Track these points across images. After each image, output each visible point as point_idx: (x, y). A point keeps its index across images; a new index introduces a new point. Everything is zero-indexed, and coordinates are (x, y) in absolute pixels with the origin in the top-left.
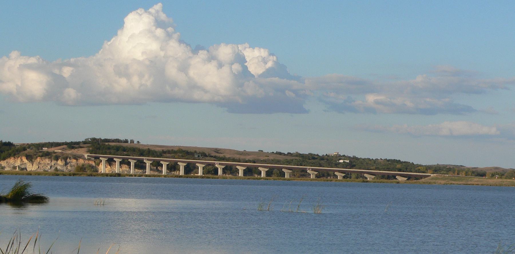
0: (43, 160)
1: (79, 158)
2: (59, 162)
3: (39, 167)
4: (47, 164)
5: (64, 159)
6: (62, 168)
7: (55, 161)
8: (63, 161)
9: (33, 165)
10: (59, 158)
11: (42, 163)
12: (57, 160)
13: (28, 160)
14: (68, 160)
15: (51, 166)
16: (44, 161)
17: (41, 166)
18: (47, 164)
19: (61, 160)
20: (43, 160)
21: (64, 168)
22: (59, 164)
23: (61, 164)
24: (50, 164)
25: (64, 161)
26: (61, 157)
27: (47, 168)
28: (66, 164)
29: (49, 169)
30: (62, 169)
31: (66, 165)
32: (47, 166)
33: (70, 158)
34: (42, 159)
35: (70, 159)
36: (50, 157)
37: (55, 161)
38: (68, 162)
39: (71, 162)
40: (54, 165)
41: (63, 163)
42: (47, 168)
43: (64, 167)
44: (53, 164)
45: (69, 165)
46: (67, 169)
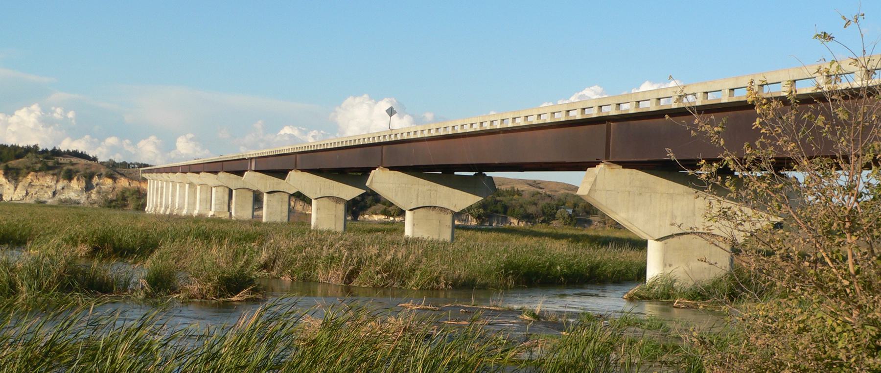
0: (41, 179)
1: (119, 176)
2: (75, 184)
3: (27, 194)
4: (47, 187)
5: (85, 177)
6: (79, 196)
7: (66, 182)
8: (81, 182)
9: (15, 190)
10: (74, 175)
11: (37, 185)
12: (70, 178)
13: (6, 178)
14: (96, 180)
15: (56, 191)
17: (32, 191)
18: (47, 187)
19: (78, 179)
20: (39, 179)
21: (83, 197)
22: (73, 187)
23: (77, 187)
24: (54, 187)
25: (84, 181)
28: (88, 188)
29: (50, 198)
30: (79, 198)
32: (46, 192)
33: (100, 176)
34: (38, 177)
35: (98, 178)
36: (56, 171)
37: (65, 181)
38: (94, 185)
40: (63, 188)
41: (80, 186)
42: (46, 196)
44: (59, 187)
45: (94, 191)
46: (88, 198)
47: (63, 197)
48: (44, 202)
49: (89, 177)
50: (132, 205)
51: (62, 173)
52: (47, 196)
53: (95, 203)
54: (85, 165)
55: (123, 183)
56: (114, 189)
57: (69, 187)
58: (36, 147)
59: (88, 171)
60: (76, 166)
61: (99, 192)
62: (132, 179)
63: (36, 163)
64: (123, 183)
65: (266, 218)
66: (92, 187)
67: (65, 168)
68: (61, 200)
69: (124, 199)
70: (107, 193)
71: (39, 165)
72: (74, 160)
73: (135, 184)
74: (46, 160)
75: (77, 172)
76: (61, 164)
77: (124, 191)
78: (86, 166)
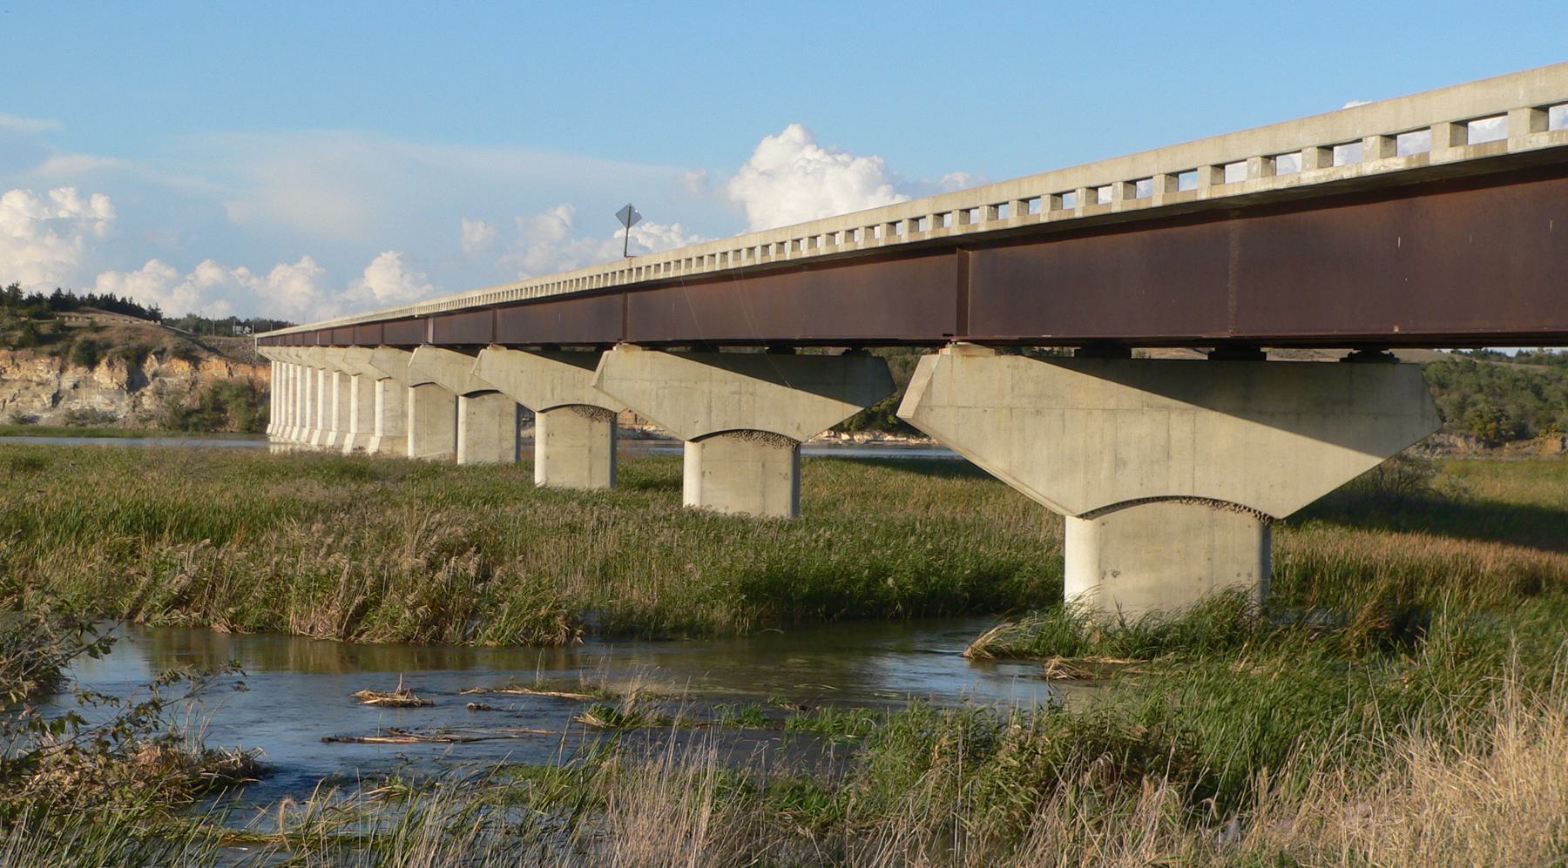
0: (23, 364)
1: (204, 354)
2: (102, 374)
4: (39, 384)
5: (127, 358)
6: (112, 402)
7: (82, 370)
8: (117, 370)
10: (99, 354)
11: (15, 380)
12: (91, 363)
14: (151, 365)
15: (58, 392)
16: (25, 371)
18: (39, 384)
19: (110, 364)
20: (18, 366)
21: (123, 404)
22: (99, 383)
23: (109, 382)
24: (54, 384)
25: (124, 369)
26: (110, 351)
27: (37, 404)
28: (135, 383)
29: (45, 410)
30: (112, 408)
31: (137, 389)
32: (37, 396)
33: (160, 355)
34: (17, 361)
35: (158, 359)
36: (59, 346)
37: (80, 369)
38: (149, 375)
39: (168, 375)
40: (76, 386)
41: (114, 380)
43: (121, 399)
44: (67, 381)
45: (148, 390)
46: (134, 407)
47: (75, 406)
48: (33, 419)
49: (136, 359)
50: (236, 421)
51: (73, 350)
52: (38, 406)
53: (152, 417)
54: (127, 328)
55: (215, 369)
56: (194, 383)
57: (89, 383)
58: (15, 290)
59: (133, 344)
60: (105, 334)
61: (159, 394)
62: (237, 360)
63: (12, 328)
64: (215, 369)
65: (466, 453)
66: (143, 382)
67: (79, 339)
68: (71, 415)
69: (219, 407)
70: (179, 393)
71: (19, 334)
72: (102, 318)
73: (243, 372)
74: (34, 321)
75: (108, 346)
76: (70, 329)
77: (218, 388)
78: (127, 334)
